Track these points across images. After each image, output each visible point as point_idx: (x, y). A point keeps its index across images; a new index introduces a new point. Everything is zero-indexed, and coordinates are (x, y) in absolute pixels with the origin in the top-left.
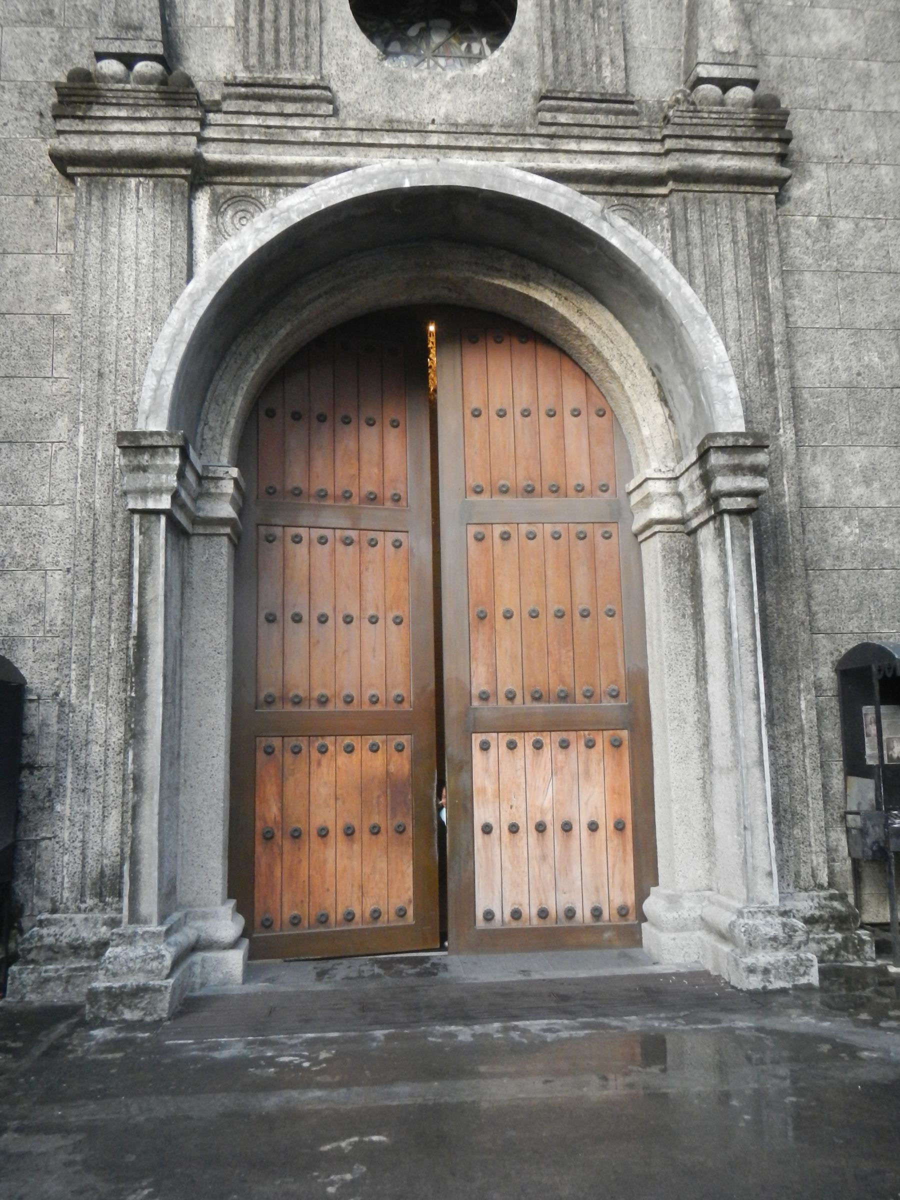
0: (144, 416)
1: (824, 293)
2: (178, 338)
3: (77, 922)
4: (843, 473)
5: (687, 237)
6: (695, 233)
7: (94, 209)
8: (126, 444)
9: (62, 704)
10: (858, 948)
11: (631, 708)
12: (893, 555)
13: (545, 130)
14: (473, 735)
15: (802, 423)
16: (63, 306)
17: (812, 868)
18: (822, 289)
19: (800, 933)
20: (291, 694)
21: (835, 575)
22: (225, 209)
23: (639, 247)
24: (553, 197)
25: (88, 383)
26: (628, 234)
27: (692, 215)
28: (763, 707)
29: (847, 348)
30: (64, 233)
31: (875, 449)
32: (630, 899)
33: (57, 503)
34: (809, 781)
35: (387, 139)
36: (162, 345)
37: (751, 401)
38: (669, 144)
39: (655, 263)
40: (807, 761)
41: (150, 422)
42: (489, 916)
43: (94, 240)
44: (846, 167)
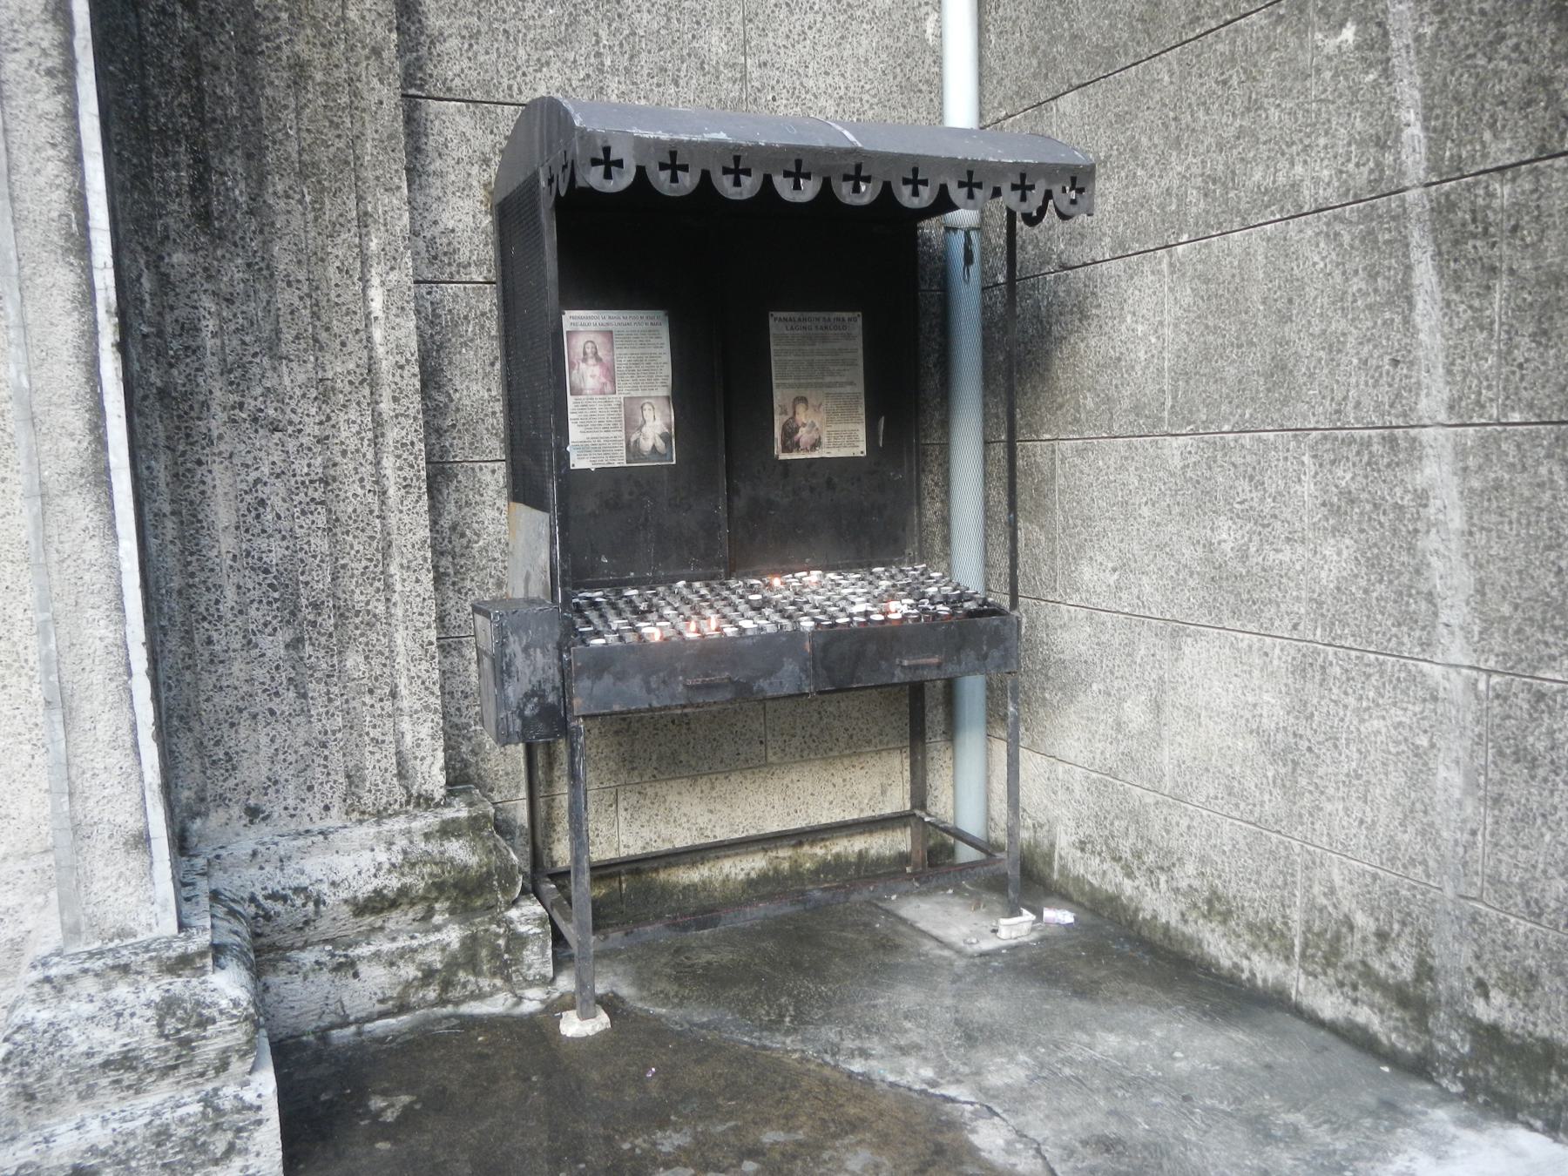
10: (505, 964)
17: (398, 753)
19: (223, 1024)
28: (105, 279)
34: (393, 520)
40: (388, 463)
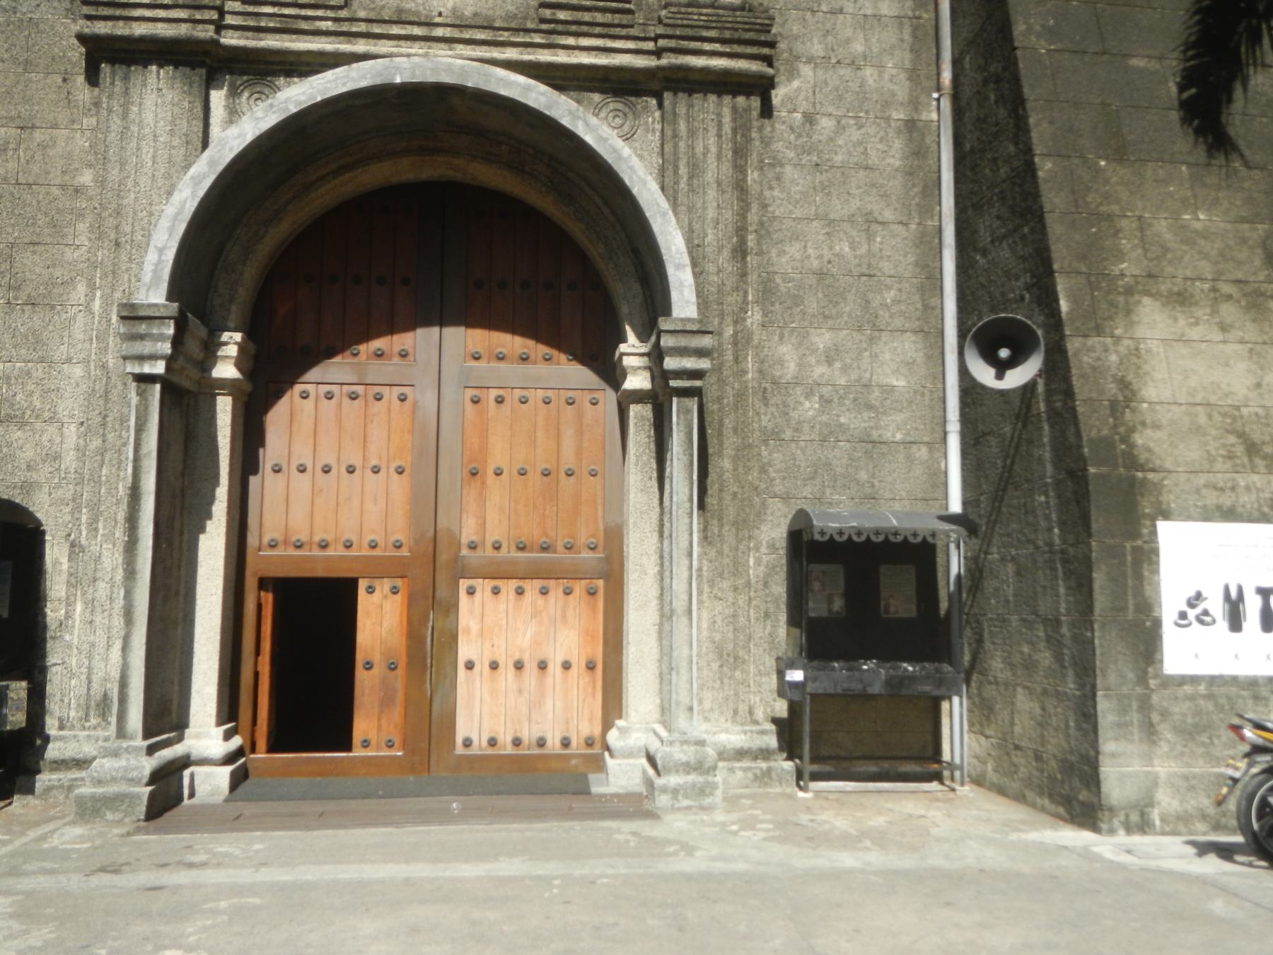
0: (145, 288)
1: (803, 186)
2: (180, 217)
3: (81, 738)
4: (807, 352)
5: (674, 131)
6: (682, 126)
7: (117, 89)
8: (125, 314)
9: (73, 545)
11: (608, 559)
12: (848, 429)
13: (544, 27)
14: (461, 581)
15: (773, 305)
16: (86, 178)
18: (801, 181)
20: (294, 539)
21: (793, 445)
22: (242, 91)
23: (610, 145)
24: (533, 95)
25: (105, 251)
26: (600, 132)
27: (682, 110)
29: (820, 237)
30: (89, 110)
31: (839, 332)
32: (597, 731)
33: (74, 361)
35: (395, 30)
36: (164, 224)
37: (723, 284)
38: (661, 43)
39: (626, 160)
40: (752, 611)
41: (151, 293)
42: (467, 743)
43: (115, 119)
44: (833, 67)
